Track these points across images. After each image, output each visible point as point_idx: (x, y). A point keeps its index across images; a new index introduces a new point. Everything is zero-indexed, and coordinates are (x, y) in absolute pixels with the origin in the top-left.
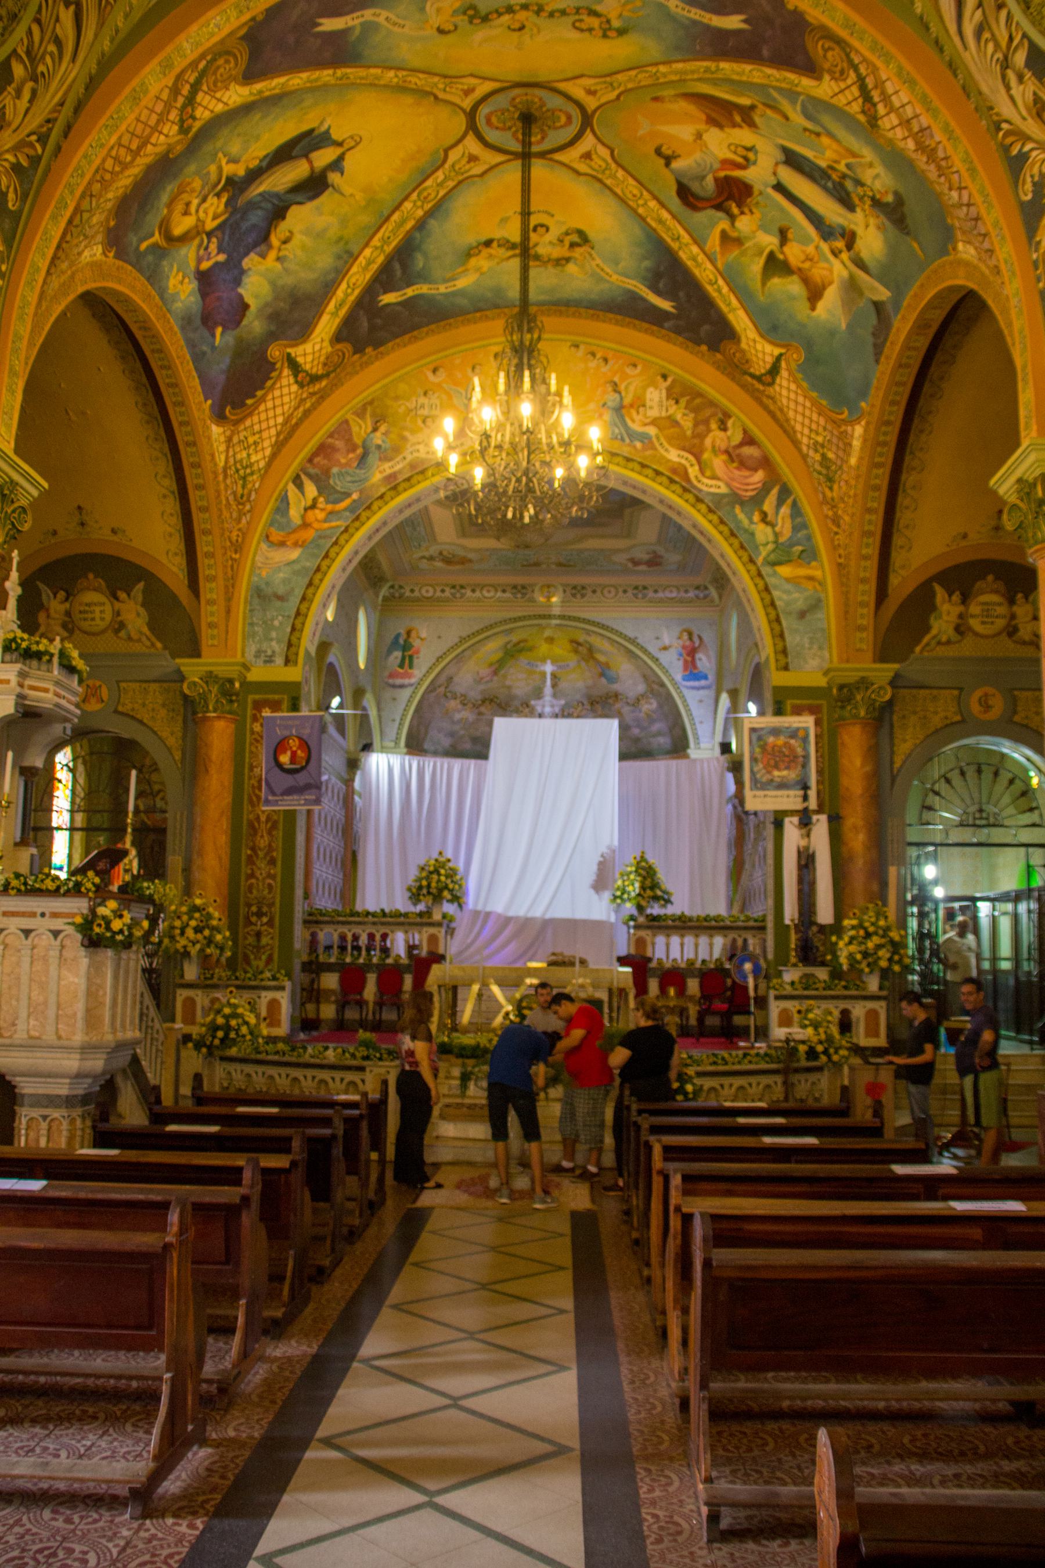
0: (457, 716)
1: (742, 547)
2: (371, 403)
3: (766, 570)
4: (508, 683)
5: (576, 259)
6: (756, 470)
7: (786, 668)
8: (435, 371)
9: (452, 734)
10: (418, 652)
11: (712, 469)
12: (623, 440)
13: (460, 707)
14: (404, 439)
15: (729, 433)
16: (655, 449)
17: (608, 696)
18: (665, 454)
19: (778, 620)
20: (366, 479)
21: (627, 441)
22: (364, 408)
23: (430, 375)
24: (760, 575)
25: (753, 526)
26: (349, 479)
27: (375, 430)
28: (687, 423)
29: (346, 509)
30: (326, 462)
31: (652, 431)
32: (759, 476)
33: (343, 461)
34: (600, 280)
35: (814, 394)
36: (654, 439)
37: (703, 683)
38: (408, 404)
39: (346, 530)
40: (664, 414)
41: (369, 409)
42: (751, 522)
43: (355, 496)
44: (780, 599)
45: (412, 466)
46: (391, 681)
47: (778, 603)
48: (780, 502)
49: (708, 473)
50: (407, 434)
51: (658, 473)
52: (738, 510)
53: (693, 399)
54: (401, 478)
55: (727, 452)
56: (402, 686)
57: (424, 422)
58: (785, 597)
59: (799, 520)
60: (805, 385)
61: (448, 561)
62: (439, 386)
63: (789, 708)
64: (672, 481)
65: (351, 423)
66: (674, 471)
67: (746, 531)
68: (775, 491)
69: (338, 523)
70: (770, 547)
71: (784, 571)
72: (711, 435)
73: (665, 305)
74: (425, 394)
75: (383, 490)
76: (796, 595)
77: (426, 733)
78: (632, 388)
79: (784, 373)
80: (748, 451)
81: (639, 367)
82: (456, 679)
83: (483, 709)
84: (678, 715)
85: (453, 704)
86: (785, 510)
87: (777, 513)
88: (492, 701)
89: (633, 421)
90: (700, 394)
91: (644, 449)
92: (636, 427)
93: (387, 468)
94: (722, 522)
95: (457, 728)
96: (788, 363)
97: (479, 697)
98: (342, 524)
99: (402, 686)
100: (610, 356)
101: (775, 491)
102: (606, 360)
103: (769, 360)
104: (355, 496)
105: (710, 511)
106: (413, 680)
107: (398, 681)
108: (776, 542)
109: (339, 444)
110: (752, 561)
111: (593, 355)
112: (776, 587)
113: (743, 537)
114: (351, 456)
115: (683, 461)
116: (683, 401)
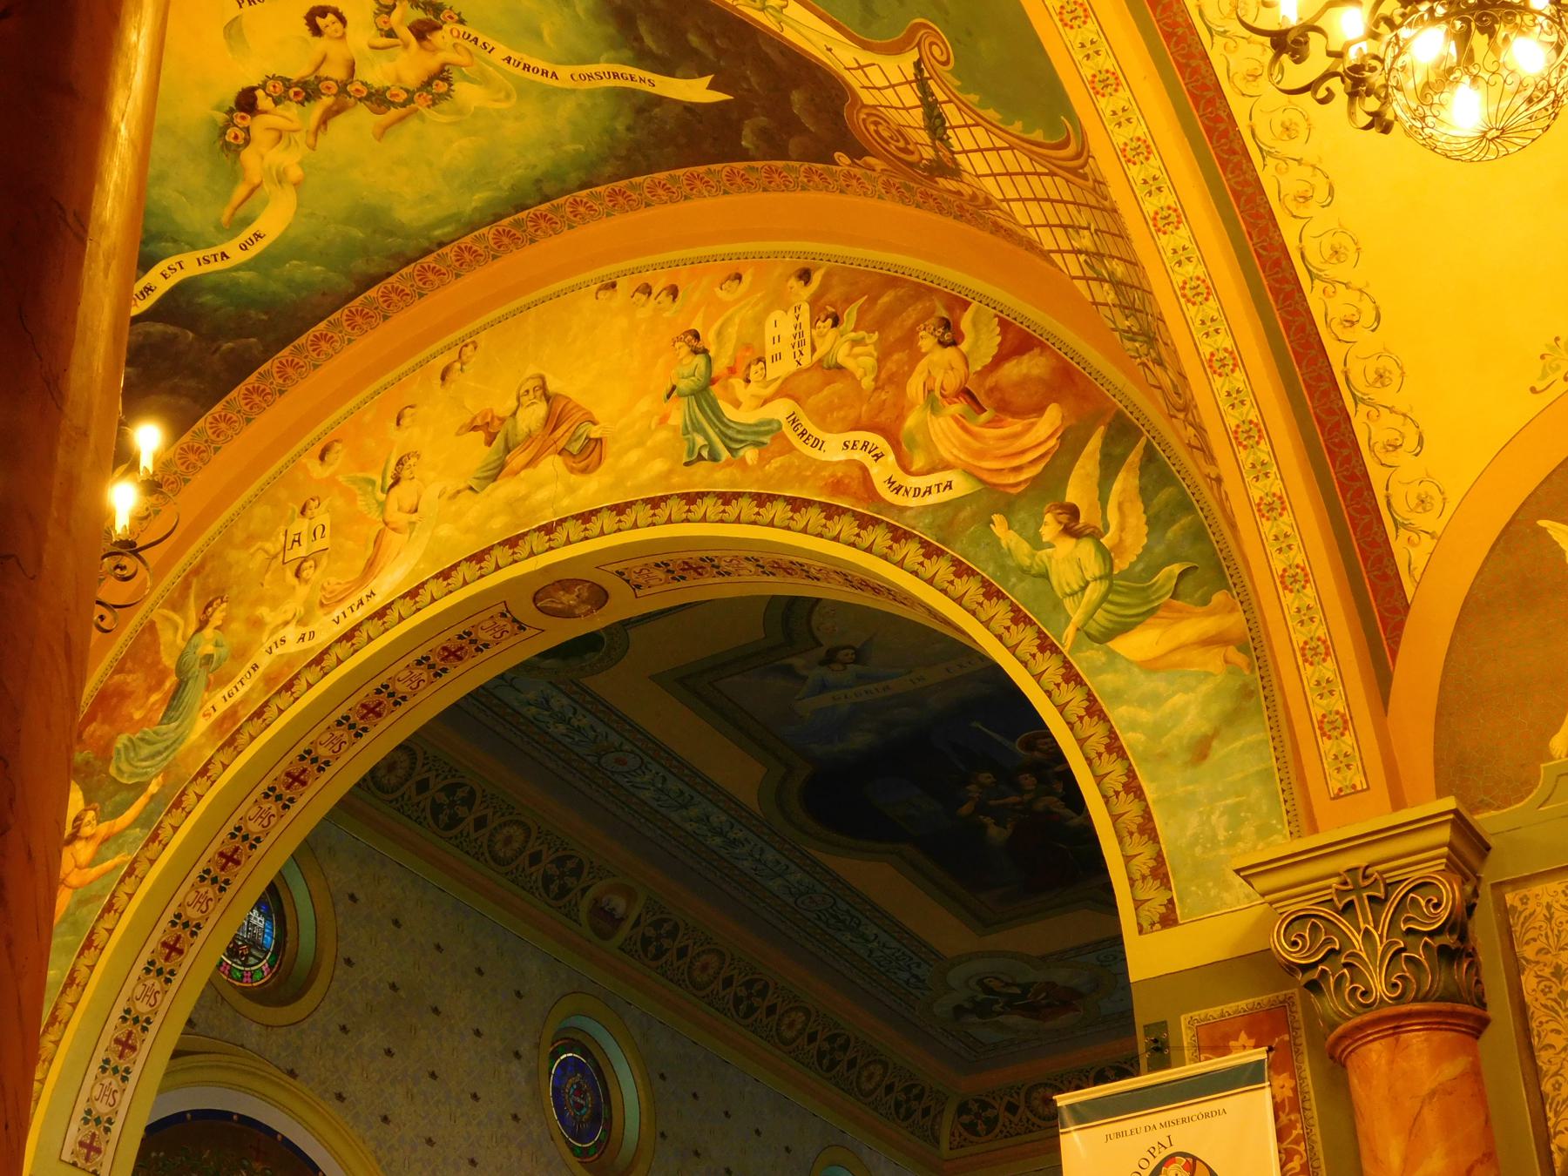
1: (1019, 617)
2: (196, 571)
3: (1086, 660)
5: (458, 66)
6: (1040, 410)
7: (1168, 920)
8: (322, 458)
11: (930, 447)
12: (714, 457)
14: (257, 624)
15: (964, 346)
16: (792, 449)
18: (814, 453)
19: (1133, 787)
20: (178, 741)
21: (725, 454)
22: (186, 585)
23: (318, 471)
24: (1071, 676)
25: (1043, 554)
26: (146, 751)
27: (203, 624)
28: (861, 361)
29: (135, 823)
30: (107, 728)
31: (780, 410)
32: (1051, 420)
33: (138, 715)
34: (547, 94)
35: (1017, 127)
36: (787, 429)
38: (268, 546)
39: (131, 871)
40: (806, 361)
41: (195, 583)
42: (1037, 543)
43: (153, 788)
44: (1133, 725)
45: (269, 680)
47: (1126, 738)
48: (1110, 466)
49: (919, 462)
50: (263, 611)
51: (796, 504)
52: (999, 526)
53: (873, 300)
54: (245, 714)
55: (966, 393)
57: (297, 574)
58: (1145, 716)
59: (1165, 495)
60: (991, 114)
61: (1032, 1010)
62: (332, 481)
63: (1187, 1038)
64: (831, 511)
65: (159, 626)
66: (837, 486)
67: (1024, 572)
68: (1095, 443)
69: (117, 860)
70: (1095, 591)
71: (1139, 644)
72: (924, 362)
73: (696, 90)
74: (303, 512)
75: (209, 753)
76: (1179, 699)
78: (732, 332)
79: (951, 113)
80: (1014, 370)
81: (747, 278)
86: (1126, 482)
87: (1104, 500)
89: (737, 404)
90: (892, 282)
91: (763, 461)
92: (742, 415)
93: (220, 701)
94: (961, 570)
96: (943, 84)
98: (122, 859)
100: (682, 278)
101: (1095, 443)
102: (674, 292)
103: (910, 97)
104: (153, 788)
105: (930, 551)
108: (1108, 576)
109: (135, 680)
110: (1046, 645)
111: (647, 290)
112: (1117, 696)
113: (1018, 591)
114: (155, 697)
115: (858, 455)
116: (850, 316)
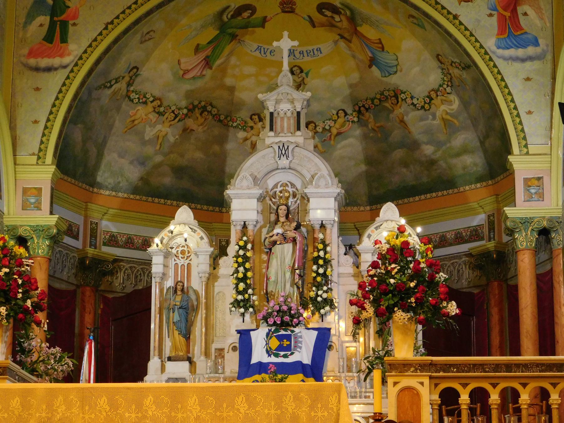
0: (149, 133)
4: (229, 81)
9: (142, 161)
10: (75, 17)
13: (153, 117)
17: (383, 98)
37: (531, 50)
46: (32, 62)
56: (49, 69)
77: (100, 155)
82: (145, 72)
83: (190, 122)
84: (497, 113)
85: (142, 111)
88: (204, 109)
95: (149, 150)
97: (184, 103)
99: (49, 69)
106: (66, 60)
107: (44, 62)
